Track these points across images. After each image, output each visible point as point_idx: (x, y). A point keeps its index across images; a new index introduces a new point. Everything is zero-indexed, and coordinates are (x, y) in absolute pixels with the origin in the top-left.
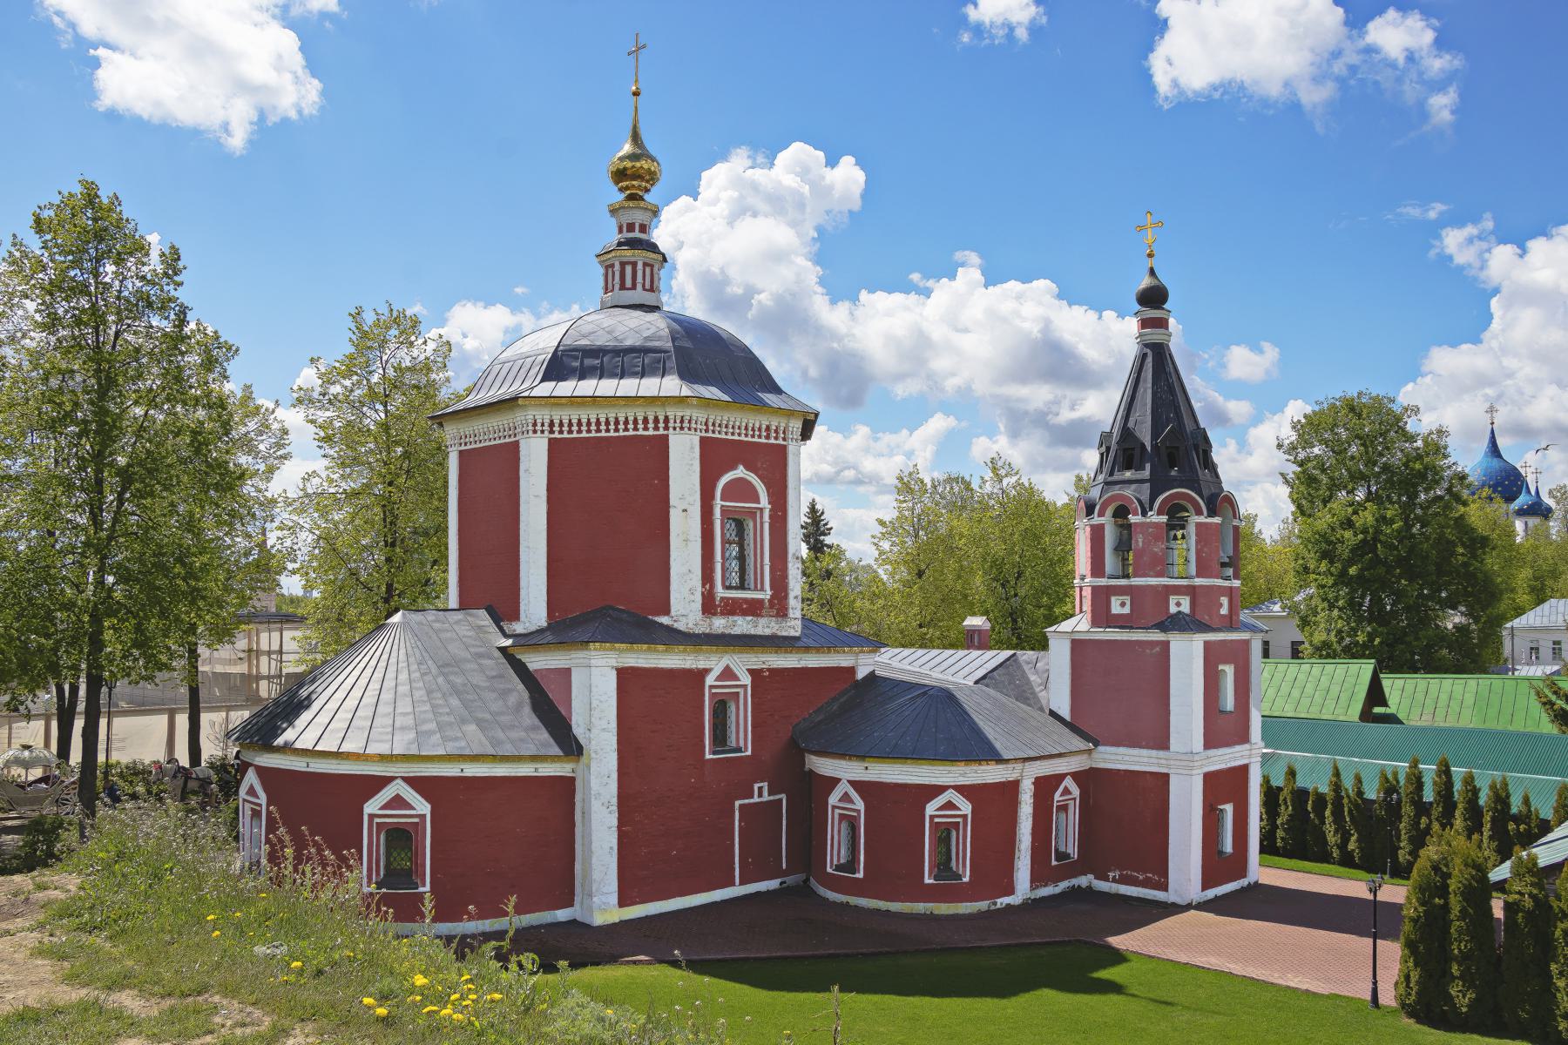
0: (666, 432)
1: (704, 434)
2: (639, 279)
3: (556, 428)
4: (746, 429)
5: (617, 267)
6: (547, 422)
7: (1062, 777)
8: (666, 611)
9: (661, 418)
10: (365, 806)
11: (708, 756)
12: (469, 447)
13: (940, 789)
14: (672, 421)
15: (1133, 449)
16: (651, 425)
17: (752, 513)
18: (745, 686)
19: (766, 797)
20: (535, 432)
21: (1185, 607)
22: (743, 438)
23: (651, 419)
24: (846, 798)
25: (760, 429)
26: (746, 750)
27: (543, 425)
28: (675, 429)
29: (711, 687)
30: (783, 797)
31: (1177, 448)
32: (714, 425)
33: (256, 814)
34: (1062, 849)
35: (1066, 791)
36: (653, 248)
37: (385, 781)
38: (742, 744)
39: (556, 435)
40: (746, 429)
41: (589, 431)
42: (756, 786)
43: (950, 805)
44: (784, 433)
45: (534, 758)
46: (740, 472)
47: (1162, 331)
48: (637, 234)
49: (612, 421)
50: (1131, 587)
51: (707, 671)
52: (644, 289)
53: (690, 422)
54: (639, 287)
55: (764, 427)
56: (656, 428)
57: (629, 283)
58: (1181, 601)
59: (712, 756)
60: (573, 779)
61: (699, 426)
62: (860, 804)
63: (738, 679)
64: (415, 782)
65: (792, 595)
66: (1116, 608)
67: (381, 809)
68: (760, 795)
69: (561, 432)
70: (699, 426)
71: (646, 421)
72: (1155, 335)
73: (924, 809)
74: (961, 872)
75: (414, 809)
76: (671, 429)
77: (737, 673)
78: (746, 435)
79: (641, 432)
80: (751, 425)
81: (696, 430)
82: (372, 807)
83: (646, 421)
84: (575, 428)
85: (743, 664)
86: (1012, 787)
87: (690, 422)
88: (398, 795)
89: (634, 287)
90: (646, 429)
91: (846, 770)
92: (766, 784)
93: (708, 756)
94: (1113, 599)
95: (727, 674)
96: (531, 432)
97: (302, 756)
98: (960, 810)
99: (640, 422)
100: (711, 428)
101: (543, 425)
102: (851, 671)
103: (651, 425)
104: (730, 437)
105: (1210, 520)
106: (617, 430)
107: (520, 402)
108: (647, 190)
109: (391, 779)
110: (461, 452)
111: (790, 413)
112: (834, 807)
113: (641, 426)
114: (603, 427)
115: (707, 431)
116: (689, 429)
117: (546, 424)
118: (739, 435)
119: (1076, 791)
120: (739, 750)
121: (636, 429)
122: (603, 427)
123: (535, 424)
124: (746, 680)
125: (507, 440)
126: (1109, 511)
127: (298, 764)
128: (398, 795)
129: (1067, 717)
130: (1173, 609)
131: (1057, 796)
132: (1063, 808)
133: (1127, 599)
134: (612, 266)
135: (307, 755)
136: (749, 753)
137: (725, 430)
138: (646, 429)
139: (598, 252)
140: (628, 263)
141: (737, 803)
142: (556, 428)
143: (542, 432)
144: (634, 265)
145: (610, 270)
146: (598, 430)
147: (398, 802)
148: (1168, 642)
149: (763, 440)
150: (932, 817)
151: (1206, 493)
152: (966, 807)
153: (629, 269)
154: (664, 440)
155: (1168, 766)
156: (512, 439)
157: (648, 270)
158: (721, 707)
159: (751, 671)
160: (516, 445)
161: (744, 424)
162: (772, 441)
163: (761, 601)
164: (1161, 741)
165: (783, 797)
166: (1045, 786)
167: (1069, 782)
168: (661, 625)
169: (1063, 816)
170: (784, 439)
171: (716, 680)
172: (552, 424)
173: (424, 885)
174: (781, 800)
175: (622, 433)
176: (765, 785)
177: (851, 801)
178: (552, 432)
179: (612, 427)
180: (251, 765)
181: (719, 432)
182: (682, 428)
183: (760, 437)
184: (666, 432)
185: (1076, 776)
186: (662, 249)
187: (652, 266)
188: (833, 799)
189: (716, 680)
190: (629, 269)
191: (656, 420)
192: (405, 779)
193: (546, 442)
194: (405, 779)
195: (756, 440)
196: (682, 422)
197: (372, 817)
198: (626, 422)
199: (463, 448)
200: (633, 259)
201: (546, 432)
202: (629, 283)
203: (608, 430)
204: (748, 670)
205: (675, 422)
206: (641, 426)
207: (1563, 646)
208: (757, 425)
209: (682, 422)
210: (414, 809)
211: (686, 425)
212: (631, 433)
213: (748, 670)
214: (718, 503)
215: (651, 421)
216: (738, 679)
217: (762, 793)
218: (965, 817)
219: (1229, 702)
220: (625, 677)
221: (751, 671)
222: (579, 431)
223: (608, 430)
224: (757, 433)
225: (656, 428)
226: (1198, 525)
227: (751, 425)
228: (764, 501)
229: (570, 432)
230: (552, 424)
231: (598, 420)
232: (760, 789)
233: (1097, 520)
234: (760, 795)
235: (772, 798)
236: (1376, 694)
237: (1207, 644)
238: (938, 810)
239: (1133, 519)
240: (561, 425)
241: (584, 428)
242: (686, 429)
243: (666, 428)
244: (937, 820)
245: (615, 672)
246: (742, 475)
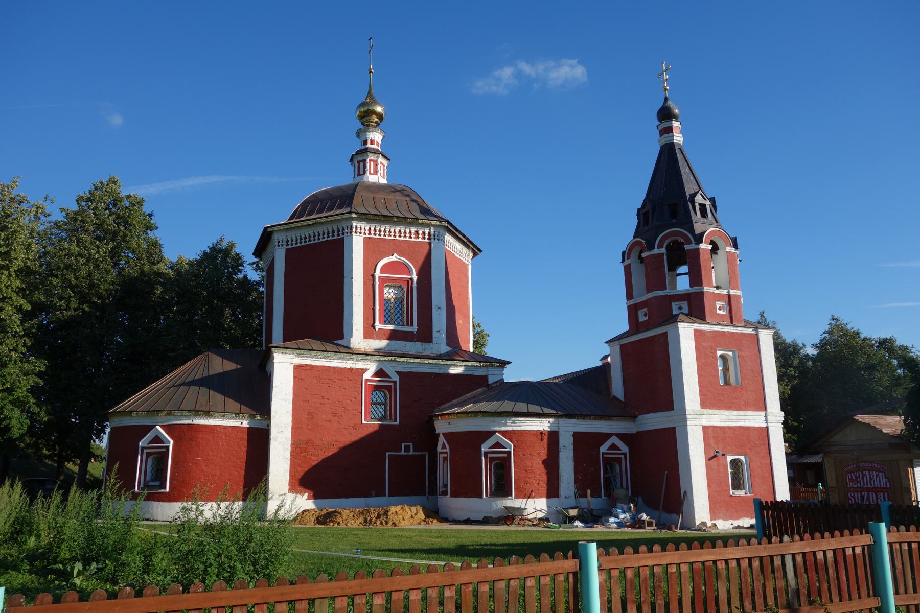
0: (343, 236)
1: (367, 236)
6: (285, 240)
7: (608, 436)
8: (342, 338)
19: (411, 453)
20: (279, 246)
24: (444, 447)
26: (395, 420)
35: (613, 447)
39: (290, 246)
42: (403, 444)
43: (498, 445)
46: (395, 258)
49: (317, 234)
51: (364, 371)
52: (370, 173)
55: (413, 232)
56: (338, 235)
58: (682, 306)
61: (363, 231)
62: (448, 450)
65: (435, 329)
66: (642, 318)
76: (345, 234)
77: (389, 373)
81: (360, 233)
89: (365, 173)
90: (333, 236)
92: (411, 444)
96: (277, 246)
101: (283, 242)
112: (440, 453)
116: (356, 233)
118: (395, 236)
119: (624, 449)
123: (279, 242)
124: (396, 378)
131: (604, 449)
136: (397, 423)
138: (333, 236)
141: (388, 454)
143: (282, 245)
144: (364, 161)
153: (362, 164)
154: (343, 238)
159: (398, 373)
163: (413, 332)
167: (614, 440)
174: (425, 456)
176: (411, 444)
178: (288, 245)
181: (380, 235)
182: (351, 233)
184: (343, 236)
185: (621, 436)
188: (439, 449)
190: (362, 164)
193: (285, 250)
196: (351, 229)
201: (284, 246)
202: (362, 172)
204: (396, 372)
205: (347, 230)
213: (396, 372)
214: (378, 274)
220: (298, 368)
221: (398, 373)
230: (287, 241)
232: (407, 449)
233: (627, 262)
235: (416, 453)
237: (696, 331)
238: (491, 448)
240: (292, 241)
243: (343, 234)
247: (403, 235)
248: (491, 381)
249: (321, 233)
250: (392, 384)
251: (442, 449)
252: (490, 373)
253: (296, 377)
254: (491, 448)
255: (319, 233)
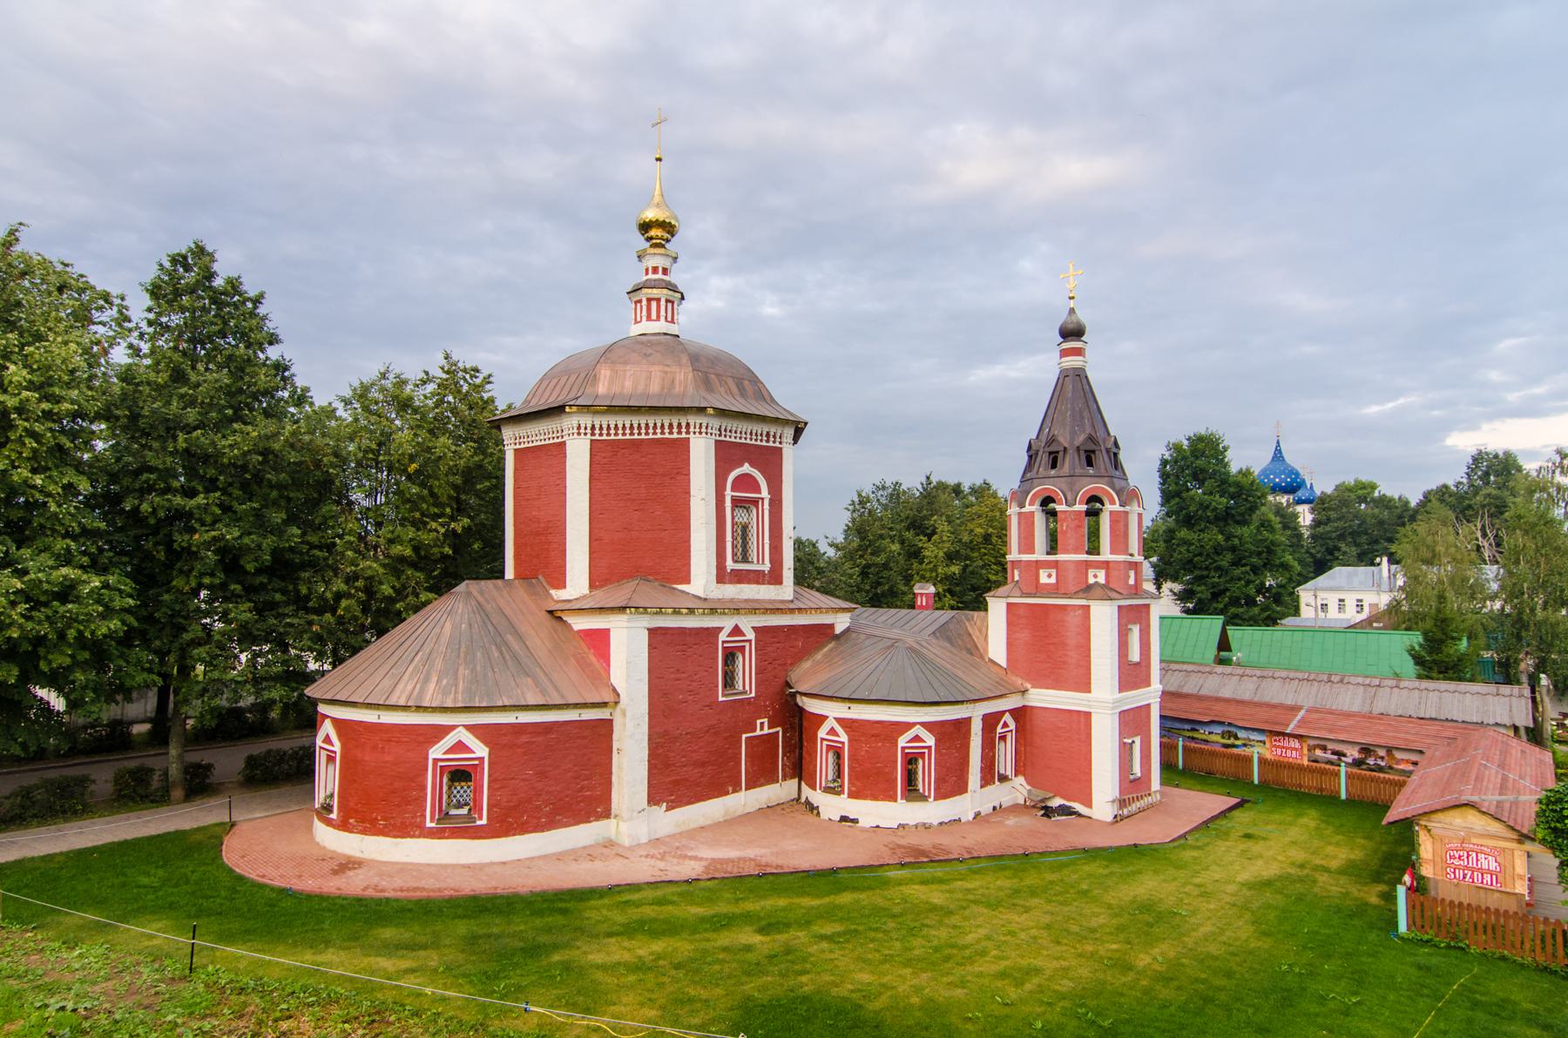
1: (718, 438)
2: (663, 313)
3: (597, 432)
4: (751, 434)
5: (644, 303)
6: (589, 426)
7: (1004, 712)
8: (687, 581)
9: (684, 425)
10: (430, 751)
11: (721, 699)
12: (522, 446)
13: (910, 726)
14: (692, 427)
15: (1057, 452)
16: (675, 430)
17: (755, 502)
18: (750, 641)
19: (766, 731)
20: (579, 434)
21: (1101, 579)
22: (748, 441)
23: (675, 425)
24: (832, 731)
25: (761, 435)
26: (751, 692)
27: (586, 428)
28: (695, 433)
29: (724, 642)
30: (779, 729)
31: (1094, 452)
32: (725, 430)
33: (331, 759)
34: (1002, 771)
35: (1005, 725)
36: (672, 288)
37: (446, 730)
38: (747, 688)
39: (597, 437)
40: (751, 434)
41: (624, 434)
42: (759, 722)
43: (917, 738)
44: (780, 437)
45: (576, 706)
46: (746, 468)
47: (1081, 358)
48: (660, 276)
49: (643, 426)
50: (1057, 561)
51: (720, 629)
53: (707, 428)
54: (662, 318)
55: (765, 433)
56: (680, 432)
57: (654, 316)
59: (724, 699)
60: (611, 721)
61: (714, 431)
62: (844, 737)
63: (744, 635)
64: (471, 728)
66: (1044, 578)
67: (444, 753)
68: (762, 729)
69: (601, 435)
70: (714, 431)
71: (671, 426)
72: (1072, 362)
73: (897, 741)
74: (927, 794)
75: (473, 752)
78: (751, 439)
79: (667, 436)
80: (754, 432)
82: (437, 752)
83: (671, 426)
84: (612, 432)
85: (748, 624)
86: (968, 721)
87: (707, 428)
88: (460, 742)
90: (671, 433)
91: (833, 711)
92: (766, 720)
93: (721, 699)
94: (1041, 571)
95: (737, 631)
97: (375, 709)
98: (924, 742)
99: (666, 427)
100: (723, 433)
101: (586, 428)
102: (831, 626)
103: (675, 430)
104: (738, 440)
105: (1122, 509)
106: (647, 434)
107: (567, 409)
108: (668, 241)
109: (453, 728)
110: (515, 450)
111: (785, 422)
112: (822, 739)
113: (667, 430)
114: (636, 431)
115: (720, 435)
116: (707, 433)
117: (589, 428)
118: (746, 439)
119: (1012, 726)
120: (745, 693)
121: (663, 433)
122: (636, 431)
123: (579, 428)
124: (751, 635)
125: (556, 441)
126: (1038, 502)
127: (369, 716)
128: (460, 742)
129: (1004, 665)
130: (1091, 580)
131: (999, 730)
132: (1003, 738)
133: (1054, 572)
134: (640, 301)
135: (378, 709)
136: (753, 695)
137: (734, 435)
138: (671, 433)
139: (629, 290)
140: (653, 299)
141: (744, 736)
142: (597, 432)
143: (586, 434)
144: (658, 300)
145: (639, 305)
146: (632, 434)
147: (460, 746)
148: (1089, 606)
149: (764, 443)
150: (903, 748)
151: (1117, 487)
152: (930, 741)
153: (654, 304)
155: (1089, 706)
156: (560, 440)
157: (670, 305)
158: (730, 656)
159: (754, 628)
160: (564, 444)
161: (749, 431)
162: (771, 444)
164: (1084, 685)
165: (779, 729)
166: (991, 721)
167: (1007, 718)
168: (683, 592)
169: (1002, 744)
170: (780, 443)
171: (728, 636)
172: (593, 428)
173: (481, 818)
174: (778, 732)
175: (651, 436)
176: (766, 720)
177: (838, 736)
178: (593, 434)
179: (643, 431)
180: (328, 717)
182: (700, 433)
183: (761, 440)
186: (681, 289)
187: (673, 303)
189: (728, 636)
190: (654, 304)
191: (679, 425)
192: (468, 727)
193: (588, 442)
194: (468, 727)
195: (759, 443)
196: (701, 427)
197: (436, 761)
198: (655, 427)
199: (518, 446)
200: (656, 296)
202: (654, 316)
203: (639, 434)
206: (667, 430)
207: (1346, 602)
208: (759, 432)
209: (701, 427)
210: (473, 752)
211: (704, 430)
212: (659, 436)
214: (729, 493)
215: (675, 427)
216: (744, 635)
217: (763, 727)
218: (929, 748)
219: (1135, 656)
220: (653, 632)
221: (754, 628)
222: (616, 434)
223: (639, 434)
224: (759, 438)
225: (680, 432)
226: (1111, 512)
227: (754, 432)
228: (765, 493)
229: (608, 434)
230: (593, 428)
231: (632, 425)
232: (762, 724)
233: (1028, 508)
234: (762, 729)
235: (771, 731)
236: (1224, 644)
239: (1059, 508)
240: (601, 428)
241: (620, 432)
242: (704, 434)
243: (688, 433)
244: (907, 751)
245: (647, 632)
246: (748, 472)
247: (754, 437)
248: (838, 630)
249: (651, 425)
250: (747, 645)
251: (827, 734)
252: (838, 620)
253: (652, 646)
254: (908, 742)
255: (647, 425)
